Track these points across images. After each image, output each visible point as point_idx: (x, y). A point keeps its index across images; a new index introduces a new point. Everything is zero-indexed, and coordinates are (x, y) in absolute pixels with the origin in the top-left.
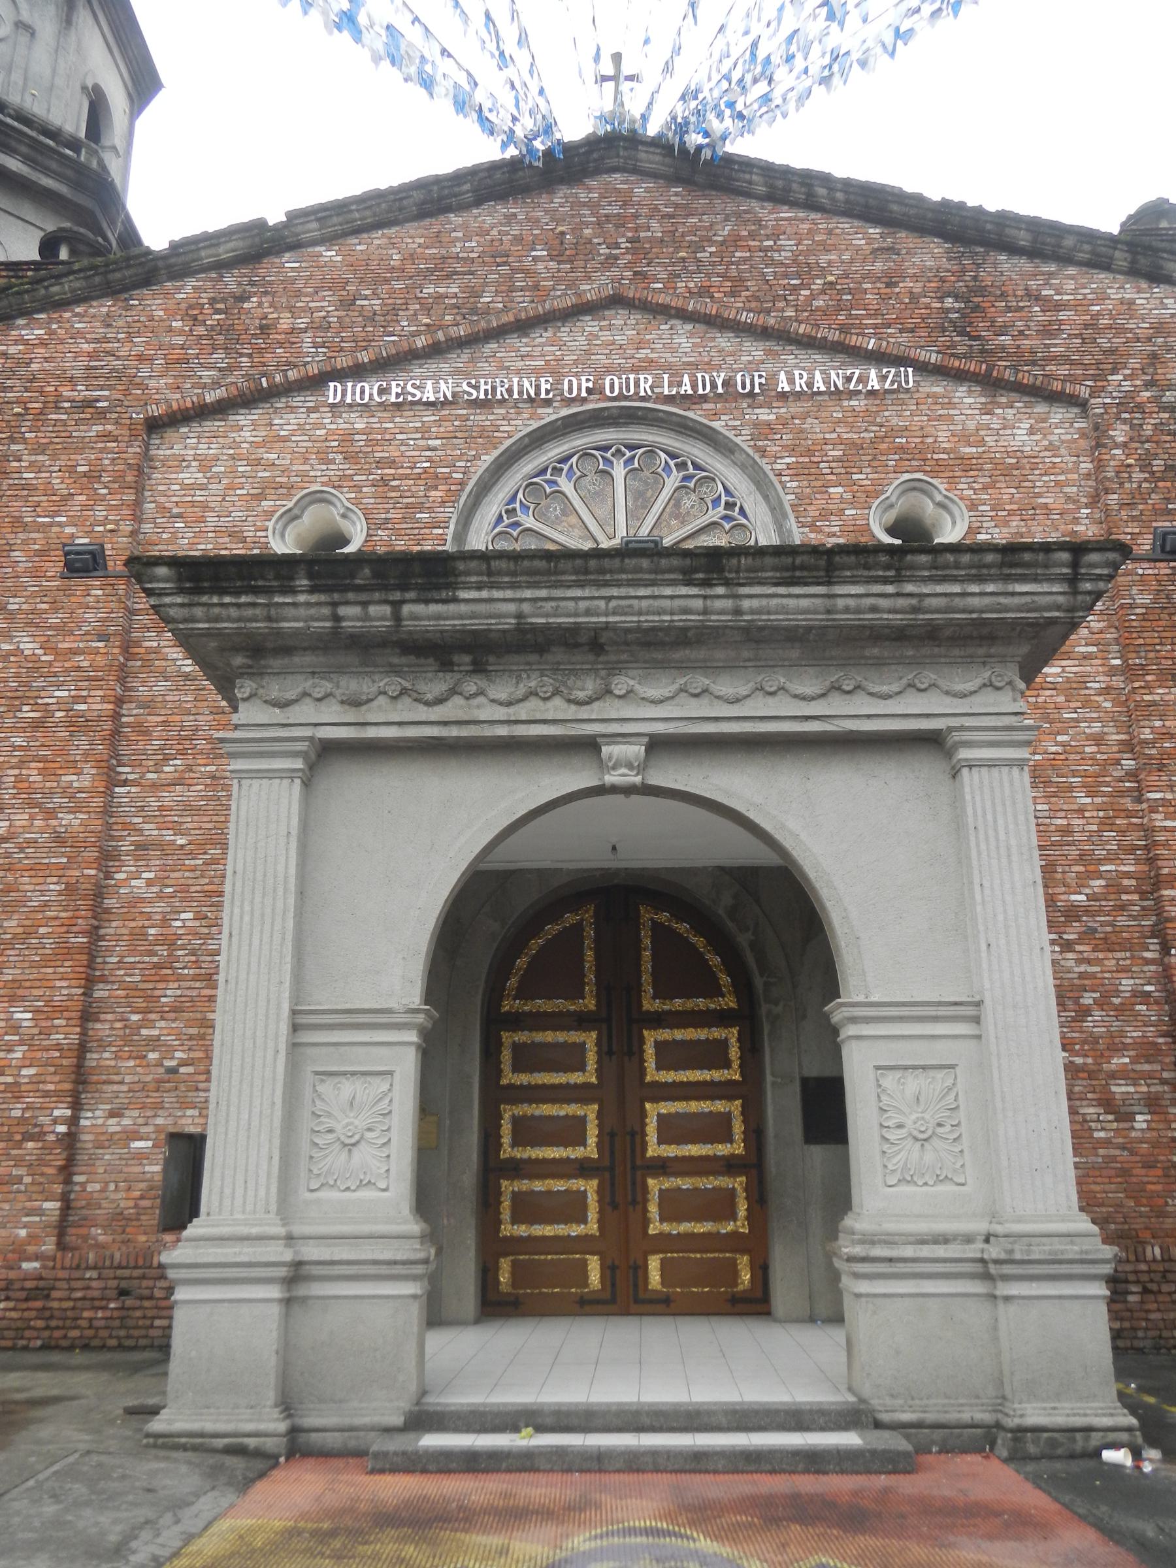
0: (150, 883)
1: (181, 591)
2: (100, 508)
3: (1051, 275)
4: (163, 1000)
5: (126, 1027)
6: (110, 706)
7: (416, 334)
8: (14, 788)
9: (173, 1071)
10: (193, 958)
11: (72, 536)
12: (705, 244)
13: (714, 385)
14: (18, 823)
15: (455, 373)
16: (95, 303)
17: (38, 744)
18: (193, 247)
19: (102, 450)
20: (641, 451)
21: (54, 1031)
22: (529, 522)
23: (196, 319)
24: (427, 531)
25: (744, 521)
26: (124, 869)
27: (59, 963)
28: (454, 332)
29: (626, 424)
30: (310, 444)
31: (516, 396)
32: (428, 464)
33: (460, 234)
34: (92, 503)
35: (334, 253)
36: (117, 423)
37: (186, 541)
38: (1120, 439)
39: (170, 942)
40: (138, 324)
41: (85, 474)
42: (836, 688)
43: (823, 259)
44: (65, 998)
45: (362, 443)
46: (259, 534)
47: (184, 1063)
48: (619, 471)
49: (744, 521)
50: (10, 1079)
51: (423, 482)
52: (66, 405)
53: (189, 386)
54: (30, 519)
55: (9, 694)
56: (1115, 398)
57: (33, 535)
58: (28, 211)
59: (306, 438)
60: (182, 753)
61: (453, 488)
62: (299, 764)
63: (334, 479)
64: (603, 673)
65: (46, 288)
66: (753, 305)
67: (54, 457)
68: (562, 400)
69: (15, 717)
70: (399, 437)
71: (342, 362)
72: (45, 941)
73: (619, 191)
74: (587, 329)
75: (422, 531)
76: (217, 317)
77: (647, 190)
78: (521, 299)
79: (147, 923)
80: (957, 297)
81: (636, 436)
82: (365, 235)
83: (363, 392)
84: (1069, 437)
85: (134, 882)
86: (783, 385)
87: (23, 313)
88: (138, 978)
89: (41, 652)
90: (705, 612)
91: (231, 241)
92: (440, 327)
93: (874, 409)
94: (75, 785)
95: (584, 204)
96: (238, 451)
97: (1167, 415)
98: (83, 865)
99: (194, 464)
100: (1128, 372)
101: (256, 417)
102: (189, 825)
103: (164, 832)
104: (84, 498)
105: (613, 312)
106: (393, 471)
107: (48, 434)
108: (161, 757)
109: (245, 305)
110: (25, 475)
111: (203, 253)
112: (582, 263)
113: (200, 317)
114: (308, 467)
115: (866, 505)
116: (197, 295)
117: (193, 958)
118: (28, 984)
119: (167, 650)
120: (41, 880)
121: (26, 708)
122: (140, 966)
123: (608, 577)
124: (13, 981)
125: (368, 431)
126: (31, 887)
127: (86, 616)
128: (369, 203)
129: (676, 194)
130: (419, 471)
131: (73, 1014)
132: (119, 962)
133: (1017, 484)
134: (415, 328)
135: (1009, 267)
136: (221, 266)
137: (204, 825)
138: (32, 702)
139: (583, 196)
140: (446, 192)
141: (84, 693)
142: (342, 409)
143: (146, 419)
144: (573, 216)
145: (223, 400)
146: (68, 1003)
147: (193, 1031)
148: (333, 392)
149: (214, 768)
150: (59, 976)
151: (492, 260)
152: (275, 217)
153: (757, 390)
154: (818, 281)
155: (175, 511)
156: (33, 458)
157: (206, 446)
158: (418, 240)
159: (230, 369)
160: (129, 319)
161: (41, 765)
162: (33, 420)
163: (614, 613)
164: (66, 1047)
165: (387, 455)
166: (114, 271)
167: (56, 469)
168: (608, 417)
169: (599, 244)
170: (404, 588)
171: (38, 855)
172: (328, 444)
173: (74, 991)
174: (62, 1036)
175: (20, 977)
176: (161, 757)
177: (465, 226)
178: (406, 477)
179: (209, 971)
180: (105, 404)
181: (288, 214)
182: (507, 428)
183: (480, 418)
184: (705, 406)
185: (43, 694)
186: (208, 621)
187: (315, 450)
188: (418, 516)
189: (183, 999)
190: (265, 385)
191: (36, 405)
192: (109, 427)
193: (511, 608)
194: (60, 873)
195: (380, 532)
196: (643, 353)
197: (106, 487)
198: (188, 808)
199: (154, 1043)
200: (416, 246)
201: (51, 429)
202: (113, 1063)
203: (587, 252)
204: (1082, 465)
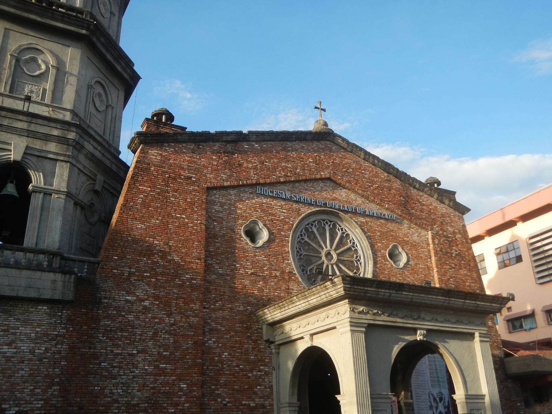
0: (214, 342)
1: (350, 284)
2: (195, 215)
3: (421, 196)
4: (221, 381)
5: (210, 390)
6: (203, 283)
7: (281, 177)
8: (175, 307)
9: (225, 405)
10: (229, 368)
11: (187, 223)
12: (350, 168)
13: (352, 209)
14: (177, 319)
15: (289, 190)
16: (189, 144)
17: (182, 293)
18: (221, 135)
19: (194, 195)
20: (332, 223)
21: (194, 391)
22: (306, 239)
23: (219, 157)
24: (284, 238)
25: (356, 248)
26: (206, 337)
27: (194, 368)
28: (290, 178)
29: (330, 215)
30: (251, 204)
31: (306, 202)
32: (283, 217)
33: (291, 149)
34: (193, 212)
35: (258, 146)
36: (198, 187)
37: (218, 229)
38: (437, 243)
39: (221, 361)
40: (203, 155)
41: (190, 202)
42: (458, 321)
43: (375, 179)
44: (196, 380)
45: (265, 207)
46: (238, 231)
47: (228, 402)
48: (327, 228)
49: (356, 248)
50: (181, 408)
51: (282, 223)
52: (183, 177)
53: (219, 179)
54: (174, 214)
55: (171, 274)
56: (435, 232)
57: (175, 220)
58: (116, 82)
59: (250, 202)
60: (221, 300)
61: (290, 226)
62: (364, 329)
63: (258, 217)
64: (418, 312)
65: (177, 136)
66: (361, 188)
67: (180, 195)
68: (316, 205)
69: (174, 283)
70: (275, 207)
71: (262, 181)
72: (189, 360)
73: (329, 147)
74: (321, 185)
75: (283, 238)
76: (226, 158)
77: (336, 149)
78: (307, 173)
79: (215, 356)
80: (403, 197)
81: (332, 219)
82: (266, 142)
83: (266, 190)
84: (425, 239)
85: (209, 342)
86: (367, 213)
87: (168, 142)
88: (213, 374)
89: (180, 261)
90: (443, 303)
91: (232, 135)
92: (288, 176)
93: (386, 223)
94: (194, 308)
95: (321, 148)
96: (231, 202)
97: (445, 238)
98: (198, 335)
99: (218, 204)
100: (437, 225)
101: (235, 192)
102: (225, 324)
103: (218, 326)
104: (190, 210)
105: (326, 181)
106: (274, 218)
107: (177, 186)
108: (215, 300)
109: (234, 156)
110: (171, 199)
111: (224, 137)
112: (321, 166)
113: (221, 157)
114: (251, 212)
115: (385, 250)
116: (219, 149)
117: (229, 368)
118: (184, 375)
119: (214, 265)
120: (186, 340)
121: (177, 280)
122: (214, 370)
123: (429, 292)
124: (180, 374)
125: (266, 203)
126: (183, 342)
127: (193, 251)
128: (270, 134)
129: (342, 152)
130: (281, 219)
131: (199, 386)
132: (207, 368)
133: (415, 250)
134: (280, 175)
135: (414, 192)
136: (228, 142)
137: (229, 324)
138: (179, 278)
139: (320, 146)
140: (289, 136)
141: (195, 277)
142: (259, 195)
143: (207, 187)
144: (318, 151)
145: (229, 186)
146: (197, 382)
147: (231, 392)
148: (258, 190)
149: (231, 306)
150: (194, 373)
151: (299, 159)
152: (245, 131)
153: (362, 213)
154: (375, 185)
155: (214, 218)
156: (173, 193)
157: (222, 199)
158: (280, 148)
159: (230, 176)
160: (199, 152)
161: (183, 300)
162: (172, 180)
163: (428, 301)
164: (198, 397)
165: (272, 212)
166: (198, 136)
167: (181, 199)
168: (327, 212)
169: (325, 161)
170: (393, 290)
171: (185, 331)
172: (256, 205)
173: (199, 378)
174: (196, 393)
175: (181, 373)
176: (215, 300)
177: (291, 147)
178: (277, 220)
179: (234, 372)
180: (194, 179)
181: (249, 131)
182: (302, 210)
183: (295, 206)
184: (349, 214)
185: (182, 275)
186: (353, 292)
187: (253, 207)
188: (281, 233)
189: (227, 381)
190: (241, 184)
191: (173, 175)
192: (197, 188)
193: (411, 297)
194: (192, 337)
195: (272, 236)
196: (334, 195)
197: (196, 208)
198: (224, 318)
199: (219, 396)
200: (279, 149)
201: (178, 184)
202: (208, 402)
203: (322, 163)
204: (428, 247)
